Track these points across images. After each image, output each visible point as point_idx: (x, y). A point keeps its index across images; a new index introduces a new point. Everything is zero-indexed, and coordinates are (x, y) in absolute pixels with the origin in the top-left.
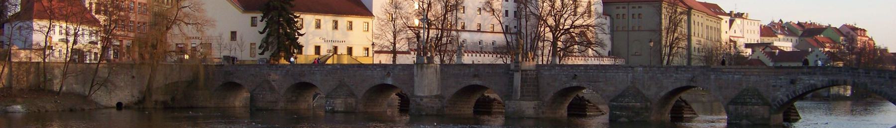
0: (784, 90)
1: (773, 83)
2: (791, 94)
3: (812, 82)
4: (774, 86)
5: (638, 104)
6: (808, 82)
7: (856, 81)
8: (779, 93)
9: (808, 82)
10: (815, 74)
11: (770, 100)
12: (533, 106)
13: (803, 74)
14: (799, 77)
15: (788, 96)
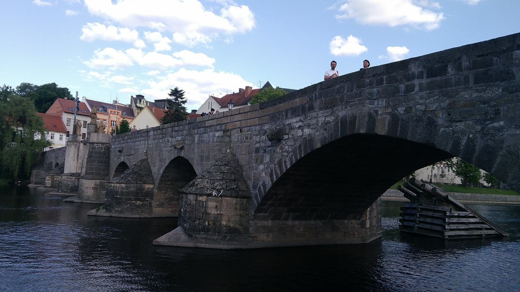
0: (267, 159)
1: (257, 142)
2: (275, 168)
3: (307, 131)
4: (257, 150)
5: (123, 185)
6: (300, 133)
7: (401, 110)
8: (261, 167)
9: (300, 133)
10: (311, 108)
11: (250, 184)
12: (93, 185)
13: (295, 112)
14: (287, 122)
15: (271, 175)
